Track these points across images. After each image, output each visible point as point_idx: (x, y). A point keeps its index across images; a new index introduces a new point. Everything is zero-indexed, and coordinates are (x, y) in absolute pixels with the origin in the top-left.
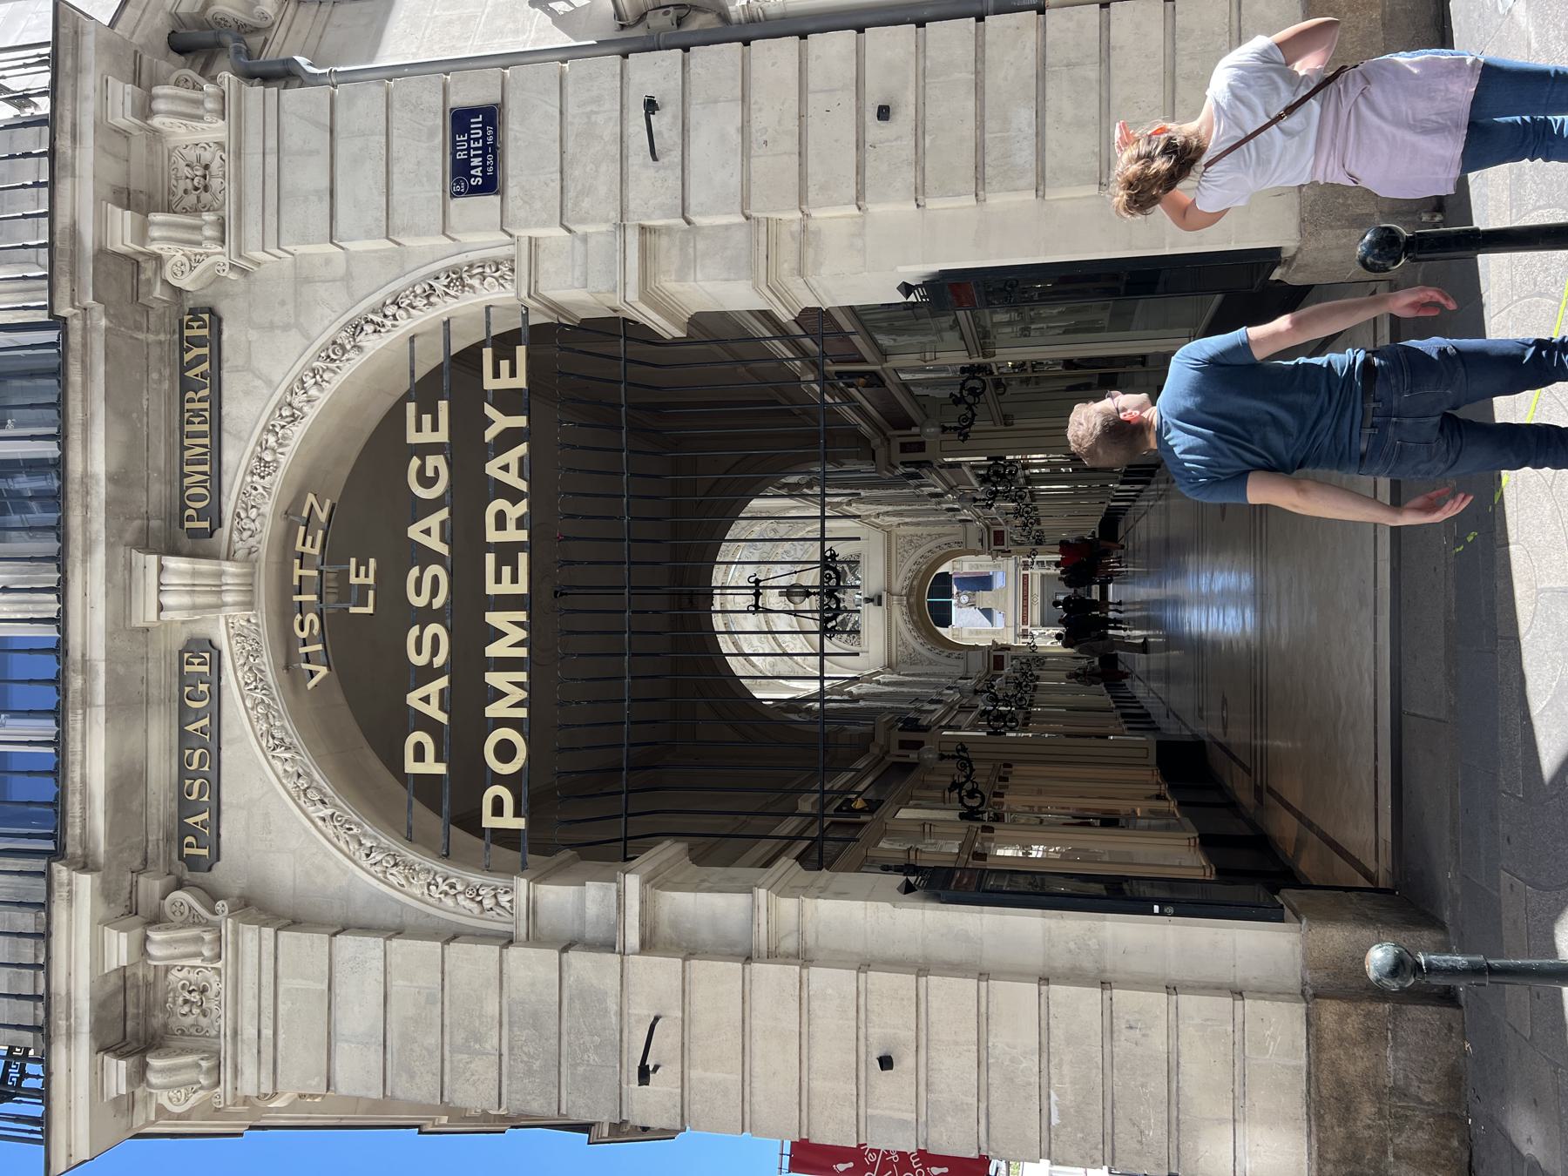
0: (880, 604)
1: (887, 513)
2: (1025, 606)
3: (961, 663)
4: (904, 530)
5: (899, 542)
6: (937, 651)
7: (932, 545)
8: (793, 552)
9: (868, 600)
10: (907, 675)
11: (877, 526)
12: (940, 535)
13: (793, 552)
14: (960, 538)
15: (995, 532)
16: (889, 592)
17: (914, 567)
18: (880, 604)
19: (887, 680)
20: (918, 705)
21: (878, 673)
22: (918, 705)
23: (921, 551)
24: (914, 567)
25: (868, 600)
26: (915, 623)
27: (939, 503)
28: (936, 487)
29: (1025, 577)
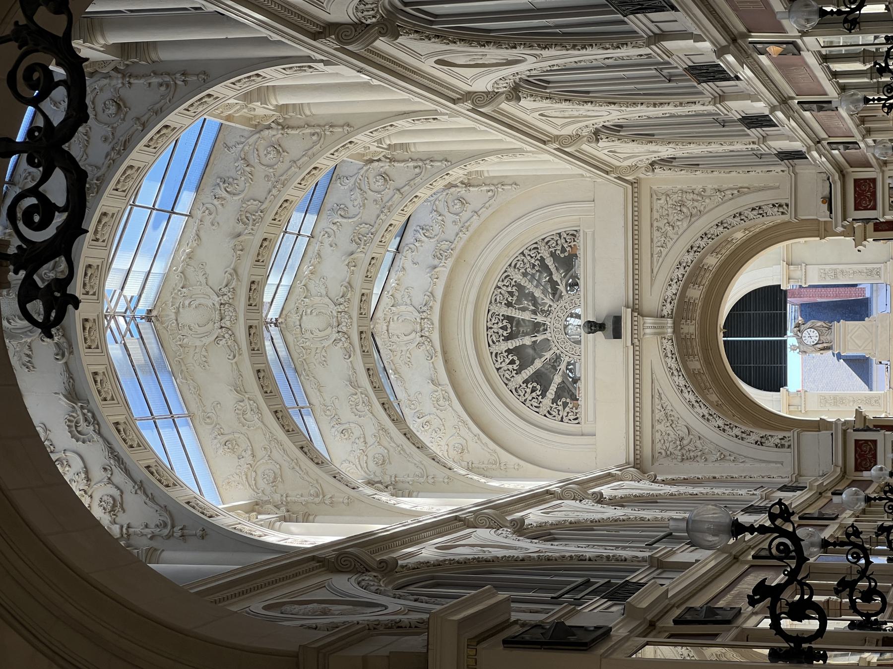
0: (617, 334)
1: (616, 130)
3: (786, 456)
4: (664, 178)
5: (657, 205)
6: (737, 431)
7: (725, 211)
8: (437, 228)
9: (594, 327)
10: (673, 482)
11: (604, 169)
12: (740, 191)
13: (437, 228)
14: (784, 196)
15: (856, 181)
16: (637, 310)
17: (689, 257)
18: (617, 334)
19: (620, 493)
20: (661, 549)
21: (609, 478)
22: (661, 549)
23: (703, 224)
24: (689, 257)
25: (594, 327)
26: (693, 377)
27: (721, 98)
28: (698, 39)
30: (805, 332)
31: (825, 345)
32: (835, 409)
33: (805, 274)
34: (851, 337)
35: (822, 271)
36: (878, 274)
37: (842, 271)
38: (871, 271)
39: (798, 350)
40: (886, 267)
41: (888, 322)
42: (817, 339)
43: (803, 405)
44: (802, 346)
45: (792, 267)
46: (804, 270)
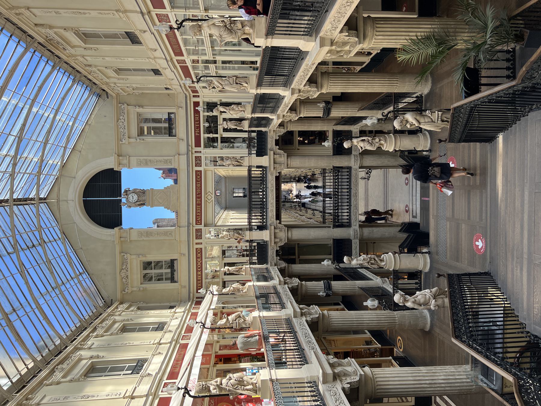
2: (199, 205)
29: (198, 174)
30: (130, 195)
31: (141, 202)
32: (147, 239)
33: (129, 162)
34: (156, 198)
35: (139, 160)
36: (170, 162)
37: (150, 161)
38: (167, 161)
39: (126, 206)
40: (174, 158)
41: (176, 189)
42: (137, 199)
43: (128, 237)
44: (128, 203)
45: (121, 158)
46: (128, 160)
